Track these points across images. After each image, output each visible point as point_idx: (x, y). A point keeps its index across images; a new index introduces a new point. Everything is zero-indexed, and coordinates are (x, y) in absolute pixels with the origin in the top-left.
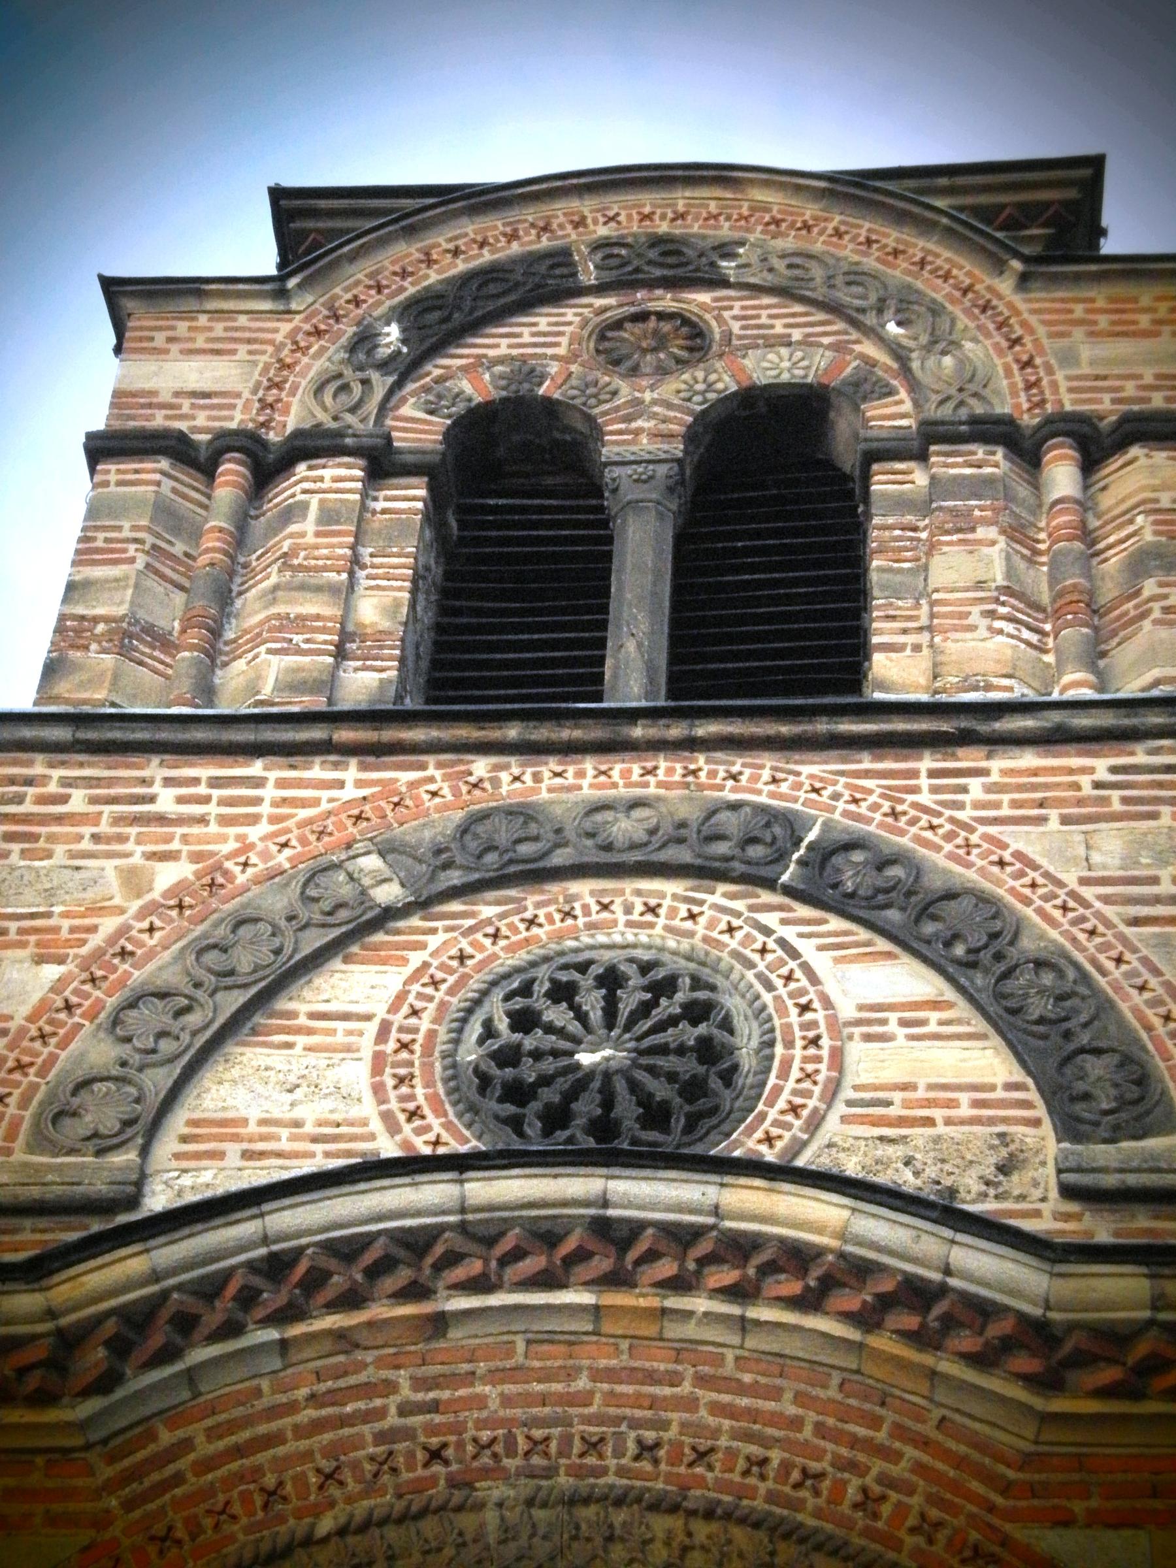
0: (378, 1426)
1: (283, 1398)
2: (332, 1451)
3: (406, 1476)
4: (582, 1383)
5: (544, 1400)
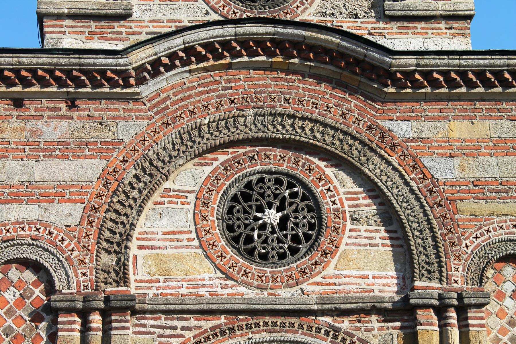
0: (217, 93)
1: (191, 85)
2: (206, 100)
3: (226, 107)
4: (268, 82)
5: (259, 86)
